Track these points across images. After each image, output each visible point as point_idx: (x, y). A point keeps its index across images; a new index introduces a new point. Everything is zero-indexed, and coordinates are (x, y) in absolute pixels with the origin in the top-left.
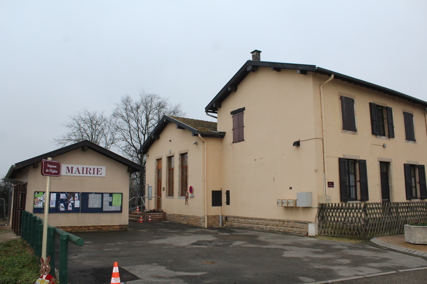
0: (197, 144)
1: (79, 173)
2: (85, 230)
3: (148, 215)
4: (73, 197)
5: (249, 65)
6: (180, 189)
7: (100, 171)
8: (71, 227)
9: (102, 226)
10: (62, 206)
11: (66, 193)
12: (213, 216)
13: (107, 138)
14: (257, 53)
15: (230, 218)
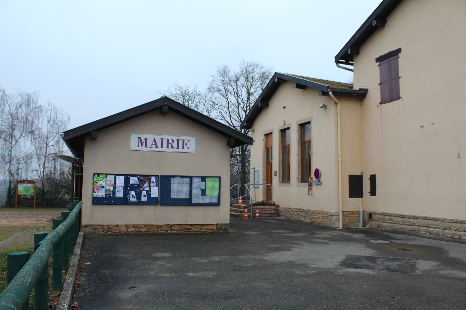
0: (325, 108)
1: (157, 147)
2: (167, 231)
3: (254, 209)
4: (148, 182)
6: (300, 172)
7: (186, 144)
8: (146, 226)
9: (191, 225)
10: (133, 195)
11: (138, 176)
12: (351, 213)
15: (376, 215)
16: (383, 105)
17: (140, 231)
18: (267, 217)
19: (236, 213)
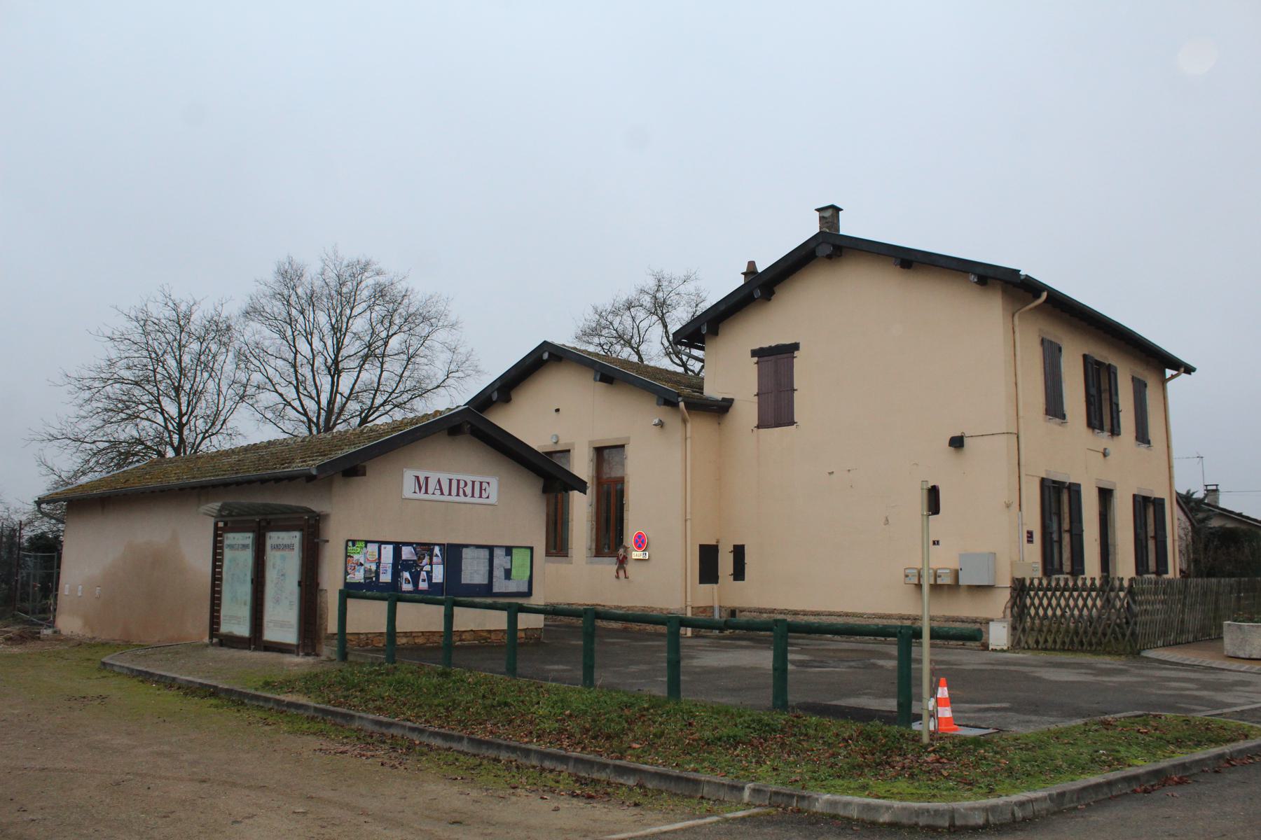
0: (662, 427)
5: (822, 242)
6: (594, 537)
7: (485, 490)
9: (489, 631)
11: (414, 546)
13: (219, 380)
14: (830, 214)
16: (762, 431)
17: (415, 643)
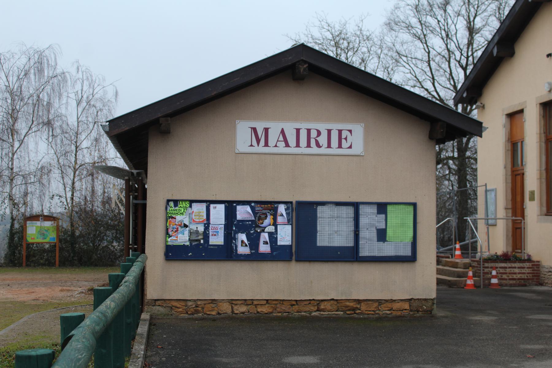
1: (287, 145)
2: (310, 312)
3: (487, 269)
4: (271, 215)
7: (346, 139)
8: (269, 301)
9: (359, 301)
10: (242, 242)
11: (253, 204)
17: (258, 312)
18: (514, 285)
19: (449, 276)
